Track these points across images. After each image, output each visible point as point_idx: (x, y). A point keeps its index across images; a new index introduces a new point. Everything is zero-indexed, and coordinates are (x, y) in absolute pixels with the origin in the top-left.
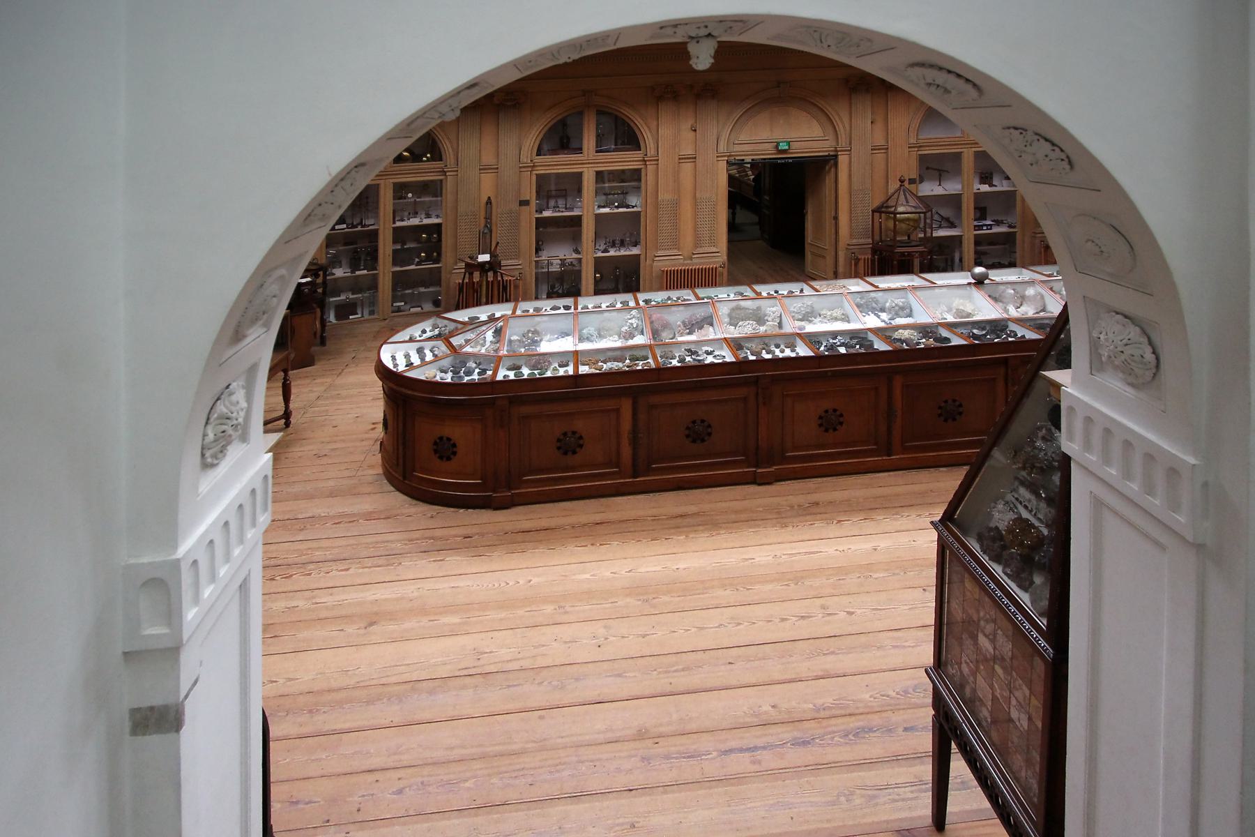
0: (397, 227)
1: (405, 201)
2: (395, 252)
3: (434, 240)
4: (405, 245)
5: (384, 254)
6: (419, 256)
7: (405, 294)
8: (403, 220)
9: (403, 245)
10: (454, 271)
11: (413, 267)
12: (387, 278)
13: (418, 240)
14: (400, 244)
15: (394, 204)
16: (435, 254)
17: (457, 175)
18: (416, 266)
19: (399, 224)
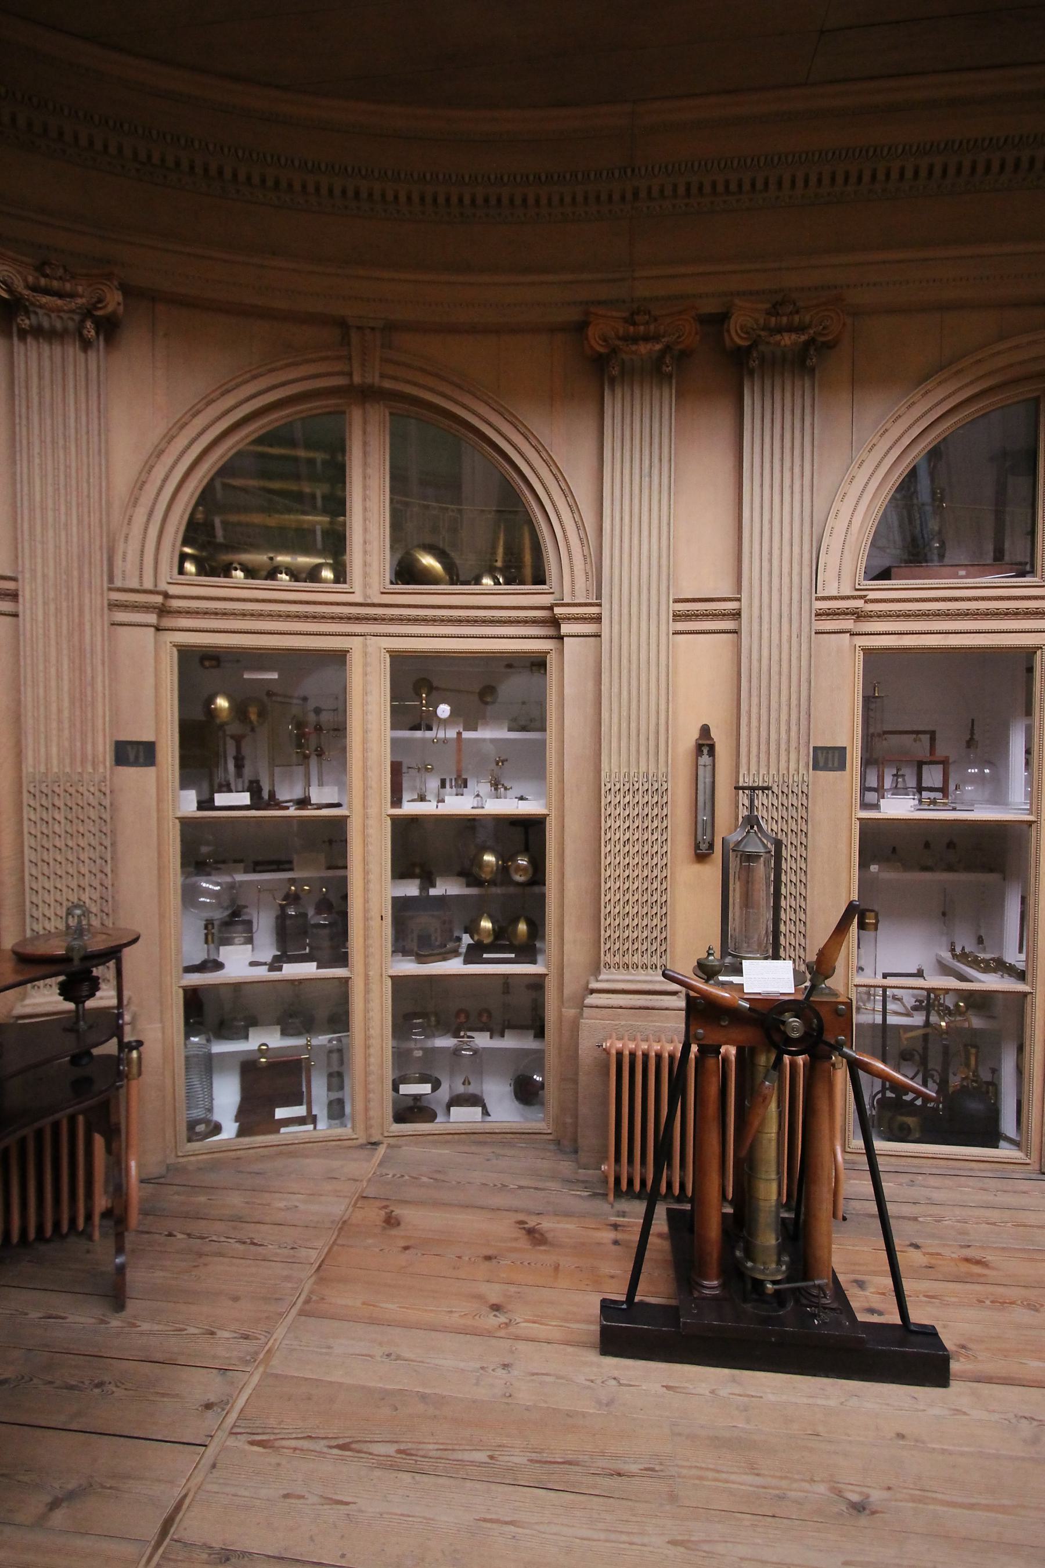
0: (414, 820)
1: (429, 734)
2: (400, 905)
3: (519, 878)
4: (434, 886)
5: (366, 911)
6: (472, 928)
7: (434, 1050)
8: (422, 798)
9: (424, 888)
10: (591, 1000)
11: (454, 966)
12: (375, 995)
13: (470, 875)
14: (417, 882)
15: (394, 742)
16: (522, 927)
17: (598, 636)
18: (466, 962)
19: (410, 808)
